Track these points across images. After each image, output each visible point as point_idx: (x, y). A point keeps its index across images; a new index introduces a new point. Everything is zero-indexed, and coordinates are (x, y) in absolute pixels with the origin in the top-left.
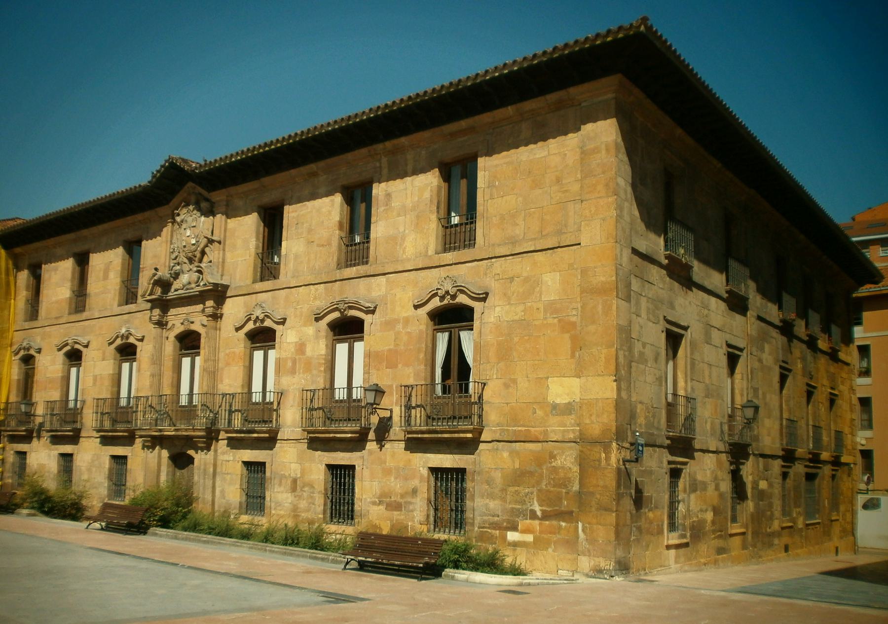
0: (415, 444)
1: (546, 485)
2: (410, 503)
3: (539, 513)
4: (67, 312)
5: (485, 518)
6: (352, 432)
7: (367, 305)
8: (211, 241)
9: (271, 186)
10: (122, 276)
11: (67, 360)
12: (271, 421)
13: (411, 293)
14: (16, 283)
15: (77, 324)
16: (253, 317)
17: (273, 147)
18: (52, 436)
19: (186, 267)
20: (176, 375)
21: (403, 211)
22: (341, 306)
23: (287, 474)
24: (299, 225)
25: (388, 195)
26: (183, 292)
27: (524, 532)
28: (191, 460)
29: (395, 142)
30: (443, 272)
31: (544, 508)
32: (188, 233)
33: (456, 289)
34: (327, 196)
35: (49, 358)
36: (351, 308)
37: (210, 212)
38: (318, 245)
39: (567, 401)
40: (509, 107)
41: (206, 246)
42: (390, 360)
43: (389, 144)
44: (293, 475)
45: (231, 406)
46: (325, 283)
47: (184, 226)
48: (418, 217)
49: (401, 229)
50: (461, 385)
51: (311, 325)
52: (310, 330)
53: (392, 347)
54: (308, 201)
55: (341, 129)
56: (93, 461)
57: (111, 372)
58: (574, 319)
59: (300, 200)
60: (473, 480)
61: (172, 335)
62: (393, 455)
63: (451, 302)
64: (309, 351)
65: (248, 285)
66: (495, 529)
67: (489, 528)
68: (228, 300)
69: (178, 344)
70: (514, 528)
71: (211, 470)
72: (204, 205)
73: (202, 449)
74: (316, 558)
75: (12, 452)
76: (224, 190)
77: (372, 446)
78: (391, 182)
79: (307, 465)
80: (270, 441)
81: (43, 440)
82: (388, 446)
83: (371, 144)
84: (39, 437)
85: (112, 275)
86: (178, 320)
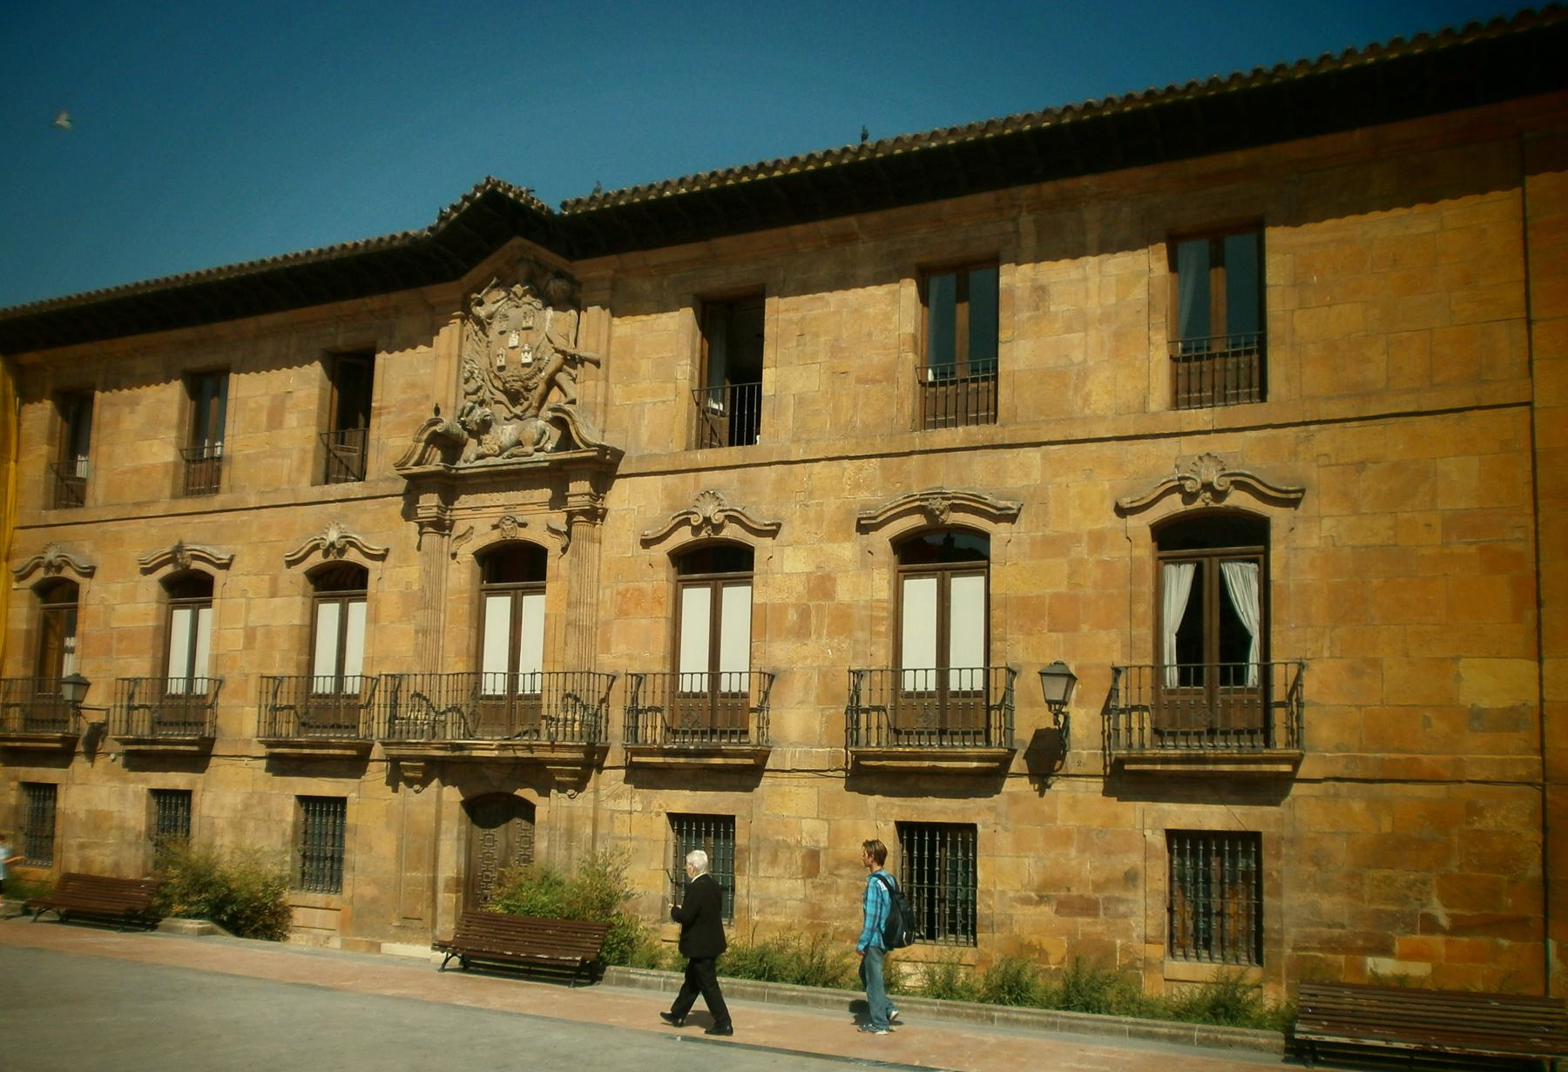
0: (1125, 780)
1: (1460, 867)
2: (1119, 900)
3: (1444, 922)
4: (167, 492)
5: (1308, 930)
6: (980, 758)
7: (1002, 504)
8: (572, 361)
9: (732, 260)
10: (319, 424)
11: (166, 594)
12: (746, 732)
13: (1107, 485)
14: (19, 425)
15: (196, 519)
16: (696, 520)
17: (777, 173)
18: (128, 754)
19: (502, 412)
20: (473, 634)
21: (1080, 321)
22: (937, 504)
23: (792, 841)
24: (808, 338)
25: (1041, 291)
26: (499, 460)
27: (1405, 957)
28: (528, 811)
29: (1067, 184)
30: (1188, 447)
31: (1455, 911)
32: (514, 340)
33: (1229, 479)
34: (879, 281)
36: (955, 508)
37: (571, 300)
38: (859, 380)
39: (1507, 702)
40: (1357, 134)
41: (559, 370)
42: (1061, 614)
43: (1048, 189)
44: (807, 842)
45: (635, 699)
46: (882, 456)
47: (497, 326)
48: (1118, 336)
49: (1077, 356)
50: (1224, 670)
51: (848, 538)
52: (847, 550)
53: (1063, 589)
54: (830, 290)
55: (962, 147)
56: (247, 807)
57: (297, 621)
58: (1515, 547)
59: (805, 288)
60: (1278, 856)
61: (467, 551)
62: (1073, 805)
63: (1212, 504)
64: (844, 592)
65: (672, 455)
66: (1334, 951)
67: (1320, 950)
68: (617, 481)
69: (478, 569)
70: (1385, 950)
71: (589, 830)
72: (556, 286)
73: (562, 788)
74: (1053, 1025)
75: (14, 784)
76: (613, 258)
77: (1017, 785)
78: (1045, 265)
79: (846, 823)
80: (747, 774)
81: (100, 762)
82: (1058, 786)
83: (1006, 185)
84: (91, 754)
85: (292, 420)
86: (482, 520)
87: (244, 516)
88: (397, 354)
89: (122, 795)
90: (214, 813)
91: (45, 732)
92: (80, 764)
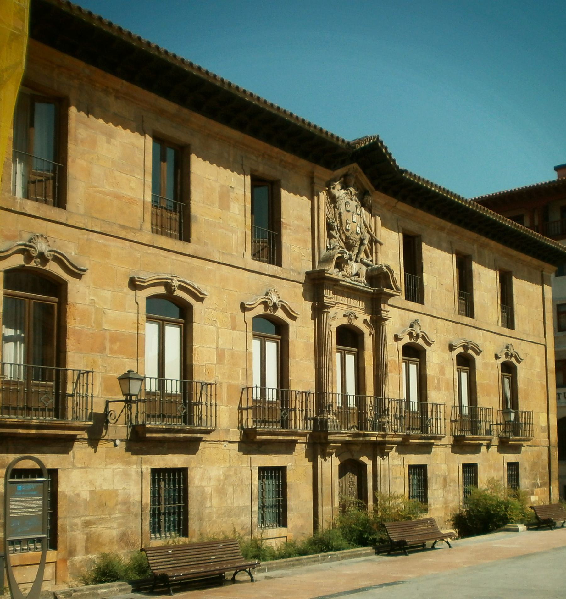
15: (174, 256)
27: (537, 495)
35: (107, 294)
56: (226, 477)
70: (533, 494)
81: (102, 447)
84: (94, 440)
87: (210, 266)
88: (292, 194)
89: (126, 474)
90: (204, 484)
91: (36, 421)
92: (80, 449)
